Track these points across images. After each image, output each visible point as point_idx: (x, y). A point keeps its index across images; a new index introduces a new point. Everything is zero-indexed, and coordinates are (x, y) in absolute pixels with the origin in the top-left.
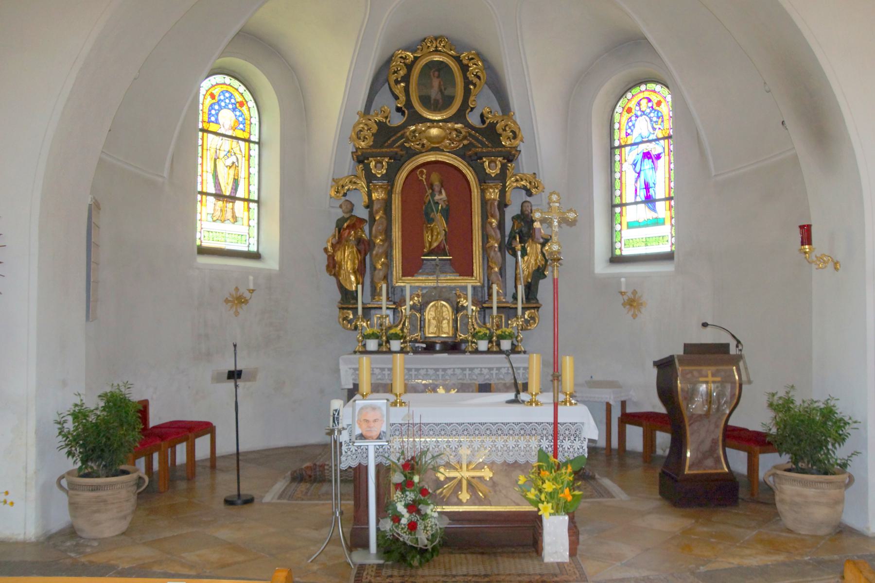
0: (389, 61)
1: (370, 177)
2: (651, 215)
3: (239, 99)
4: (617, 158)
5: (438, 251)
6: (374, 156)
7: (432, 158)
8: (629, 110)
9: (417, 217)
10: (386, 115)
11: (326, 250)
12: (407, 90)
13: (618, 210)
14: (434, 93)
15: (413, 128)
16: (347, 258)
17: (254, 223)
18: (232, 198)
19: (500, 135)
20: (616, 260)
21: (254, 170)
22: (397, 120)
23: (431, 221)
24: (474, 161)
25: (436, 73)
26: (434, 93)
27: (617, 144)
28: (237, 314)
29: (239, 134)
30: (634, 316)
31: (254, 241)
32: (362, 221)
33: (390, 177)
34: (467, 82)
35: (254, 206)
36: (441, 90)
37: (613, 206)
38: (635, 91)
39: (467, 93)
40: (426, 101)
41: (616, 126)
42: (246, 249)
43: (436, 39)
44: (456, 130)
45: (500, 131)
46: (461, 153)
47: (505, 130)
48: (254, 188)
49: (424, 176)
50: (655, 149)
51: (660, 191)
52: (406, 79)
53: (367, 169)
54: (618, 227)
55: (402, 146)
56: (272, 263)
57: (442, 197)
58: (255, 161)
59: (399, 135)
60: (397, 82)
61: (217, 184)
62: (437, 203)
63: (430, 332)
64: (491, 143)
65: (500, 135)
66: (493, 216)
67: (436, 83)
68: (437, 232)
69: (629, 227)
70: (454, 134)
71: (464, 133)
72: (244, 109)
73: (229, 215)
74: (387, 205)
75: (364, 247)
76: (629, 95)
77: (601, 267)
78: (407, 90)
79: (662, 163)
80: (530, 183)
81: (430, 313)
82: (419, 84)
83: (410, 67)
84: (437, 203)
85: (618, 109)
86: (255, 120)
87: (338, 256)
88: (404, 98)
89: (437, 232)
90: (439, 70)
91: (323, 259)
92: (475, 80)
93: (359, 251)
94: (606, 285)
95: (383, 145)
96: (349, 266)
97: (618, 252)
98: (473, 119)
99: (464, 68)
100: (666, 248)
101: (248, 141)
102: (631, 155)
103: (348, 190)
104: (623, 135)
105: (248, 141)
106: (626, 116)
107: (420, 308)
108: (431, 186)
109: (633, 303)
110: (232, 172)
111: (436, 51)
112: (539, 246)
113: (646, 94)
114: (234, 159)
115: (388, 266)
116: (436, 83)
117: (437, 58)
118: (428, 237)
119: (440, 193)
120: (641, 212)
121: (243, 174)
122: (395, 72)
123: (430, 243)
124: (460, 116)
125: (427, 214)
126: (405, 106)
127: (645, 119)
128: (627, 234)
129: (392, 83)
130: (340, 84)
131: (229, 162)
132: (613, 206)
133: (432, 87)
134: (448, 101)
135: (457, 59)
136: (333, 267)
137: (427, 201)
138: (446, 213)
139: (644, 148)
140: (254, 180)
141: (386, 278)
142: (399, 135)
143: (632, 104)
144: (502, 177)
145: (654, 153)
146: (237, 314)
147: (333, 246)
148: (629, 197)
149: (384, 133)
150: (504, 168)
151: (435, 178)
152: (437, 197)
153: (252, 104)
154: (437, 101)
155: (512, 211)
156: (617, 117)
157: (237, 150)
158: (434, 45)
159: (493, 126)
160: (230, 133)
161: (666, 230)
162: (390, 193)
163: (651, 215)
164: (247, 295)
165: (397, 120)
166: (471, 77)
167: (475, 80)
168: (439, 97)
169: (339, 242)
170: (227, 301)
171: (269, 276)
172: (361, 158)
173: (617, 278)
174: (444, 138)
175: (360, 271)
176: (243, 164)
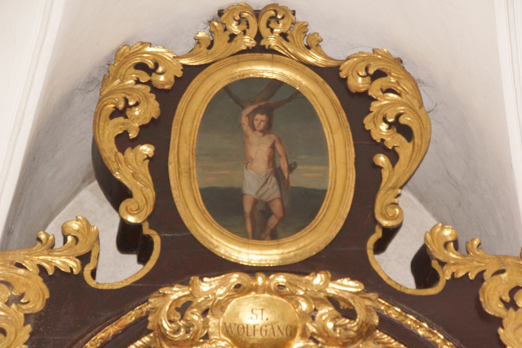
10: (82, 250)
12: (158, 167)
15: (177, 293)
19: (498, 322)
22: (118, 270)
25: (260, 118)
26: (254, 181)
34: (366, 147)
36: (277, 173)
40: (224, 205)
45: (493, 306)
52: (157, 132)
59: (129, 318)
60: (123, 142)
65: (498, 322)
67: (259, 148)
71: (361, 316)
78: (158, 167)
82: (203, 153)
83: (169, 98)
88: (151, 194)
90: (268, 111)
92: (394, 140)
98: (395, 265)
99: (355, 104)
111: (260, 49)
116: (259, 148)
122: (117, 113)
124: (348, 255)
126: (149, 219)
133: (245, 160)
134: (304, 206)
142: (129, 318)
154: (264, 210)
158: (252, 31)
165: (118, 270)
167: (394, 140)
168: (272, 192)
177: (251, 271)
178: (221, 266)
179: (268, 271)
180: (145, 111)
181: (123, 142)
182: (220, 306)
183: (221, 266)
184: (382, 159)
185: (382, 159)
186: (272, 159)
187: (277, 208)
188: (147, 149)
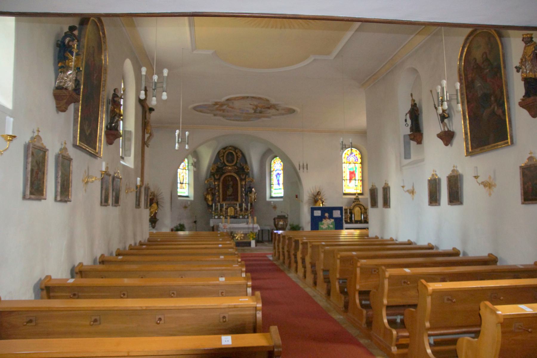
5: (231, 195)
7: (229, 174)
9: (226, 187)
16: (209, 197)
18: (183, 183)
20: (271, 197)
33: (219, 179)
37: (271, 185)
39: (237, 159)
40: (228, 161)
46: (236, 173)
52: (223, 156)
53: (214, 178)
56: (192, 198)
57: (231, 183)
64: (243, 170)
68: (230, 192)
74: (219, 185)
75: (213, 195)
77: (268, 199)
81: (229, 210)
83: (224, 153)
87: (207, 197)
89: (230, 192)
94: (269, 203)
95: (218, 170)
96: (210, 199)
99: (237, 153)
100: (282, 195)
107: (227, 209)
109: (275, 207)
115: (219, 199)
124: (235, 165)
130: (207, 158)
134: (233, 161)
135: (235, 151)
138: (232, 187)
139: (278, 172)
141: (219, 202)
144: (245, 179)
151: (230, 179)
155: (247, 187)
159: (243, 167)
162: (219, 182)
171: (191, 201)
172: (212, 174)
173: (271, 201)
175: (213, 200)
178: (227, 166)
183: (227, 166)
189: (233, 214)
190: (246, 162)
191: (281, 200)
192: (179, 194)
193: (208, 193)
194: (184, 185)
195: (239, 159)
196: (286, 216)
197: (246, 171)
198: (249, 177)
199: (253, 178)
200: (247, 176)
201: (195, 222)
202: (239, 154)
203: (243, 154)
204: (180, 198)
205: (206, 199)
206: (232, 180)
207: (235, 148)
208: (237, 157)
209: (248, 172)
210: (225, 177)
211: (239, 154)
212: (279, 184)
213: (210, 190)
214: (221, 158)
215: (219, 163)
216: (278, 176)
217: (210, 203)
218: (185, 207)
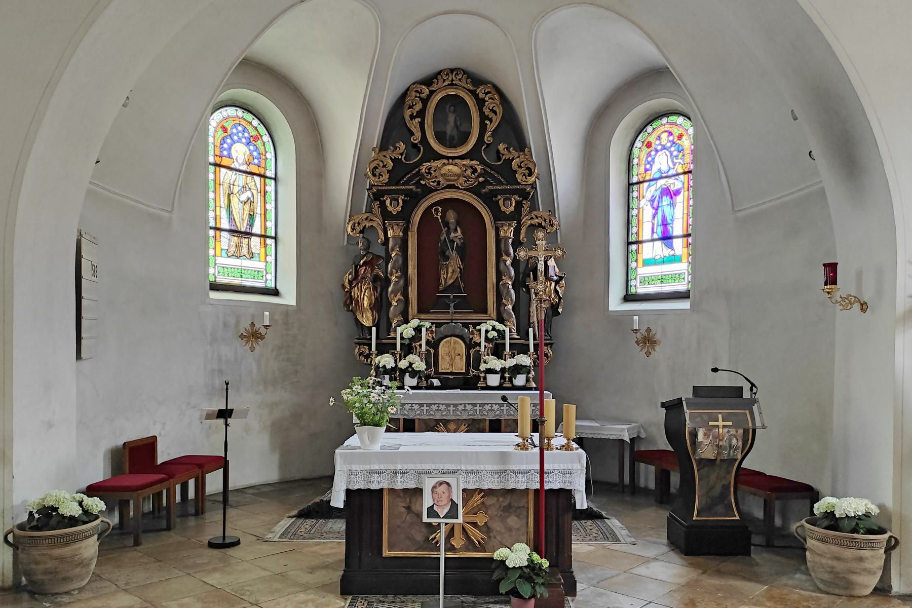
0: (404, 95)
1: (386, 215)
2: (667, 252)
3: (254, 133)
4: (635, 194)
5: (453, 287)
6: (389, 192)
8: (649, 145)
11: (343, 286)
13: (634, 247)
14: (450, 129)
15: (428, 164)
16: (365, 296)
17: (271, 259)
19: (516, 172)
21: (270, 206)
23: (447, 258)
24: (490, 200)
26: (450, 129)
27: (635, 180)
28: (252, 349)
29: (254, 169)
30: (648, 354)
31: (270, 277)
32: (379, 257)
33: (405, 216)
35: (270, 242)
36: (456, 126)
37: (630, 243)
38: (655, 124)
41: (635, 161)
42: (262, 285)
43: (452, 71)
44: (471, 167)
47: (520, 167)
48: (270, 224)
49: (440, 214)
50: (676, 184)
51: (677, 229)
52: (421, 114)
53: (383, 205)
54: (633, 265)
55: (418, 184)
56: (289, 298)
58: (271, 196)
60: (412, 117)
61: (231, 218)
62: (452, 242)
63: (444, 367)
65: (516, 172)
66: (508, 255)
67: (451, 118)
69: (646, 263)
70: (469, 172)
71: (479, 170)
72: (259, 143)
73: (245, 251)
75: (381, 283)
76: (649, 129)
77: (615, 304)
79: (679, 199)
80: (545, 221)
81: (443, 348)
82: (434, 120)
83: (425, 102)
84: (452, 242)
85: (638, 144)
86: (270, 155)
87: (356, 292)
91: (340, 296)
92: (491, 115)
93: (375, 289)
97: (633, 290)
99: (481, 103)
100: (682, 287)
101: (263, 176)
102: (649, 191)
103: (364, 227)
104: (642, 169)
105: (263, 176)
106: (646, 150)
108: (446, 224)
109: (648, 341)
110: (247, 207)
111: (452, 84)
112: (553, 284)
113: (667, 128)
114: (248, 194)
116: (451, 118)
117: (452, 92)
118: (443, 276)
119: (456, 230)
120: (657, 249)
121: (258, 211)
122: (410, 107)
123: (446, 280)
125: (443, 253)
127: (667, 154)
128: (643, 271)
129: (407, 118)
131: (244, 197)
132: (629, 243)
134: (464, 137)
135: (474, 93)
136: (350, 303)
137: (442, 238)
138: (462, 252)
140: (271, 216)
143: (652, 139)
144: (517, 215)
145: (673, 188)
146: (252, 349)
147: (350, 282)
148: (646, 234)
149: (399, 171)
150: (519, 205)
151: (451, 216)
152: (452, 235)
153: (266, 138)
154: (452, 138)
156: (636, 151)
157: (252, 185)
160: (244, 168)
161: (683, 267)
162: (406, 231)
163: (667, 252)
164: (263, 331)
166: (487, 112)
167: (491, 115)
168: (455, 133)
169: (356, 278)
170: (242, 337)
172: (377, 196)
174: (459, 176)
176: (258, 198)
177: (448, 158)
178: (440, 157)
179: (453, 158)
180: (419, 107)
181: (412, 117)
182: (440, 169)
183: (440, 157)
184: (488, 122)
185: (488, 122)
186: (455, 122)
187: (456, 137)
188: (419, 120)
189: (460, 366)
190: (521, 144)
191: (685, 305)
192: (216, 274)
193: (356, 278)
194: (255, 241)
195: (491, 127)
196: (746, 394)
197: (519, 177)
198: (534, 207)
199: (552, 212)
200: (526, 205)
201: (225, 414)
202: (492, 103)
203: (504, 100)
204: (214, 295)
205: (350, 303)
206: (458, 223)
207: (477, 81)
208: (483, 118)
209: (533, 186)
210: (428, 210)
211: (492, 103)
212: (666, 238)
213: (368, 264)
214: (414, 125)
215: (402, 146)
216: (666, 200)
217: (367, 320)
218: (254, 336)
